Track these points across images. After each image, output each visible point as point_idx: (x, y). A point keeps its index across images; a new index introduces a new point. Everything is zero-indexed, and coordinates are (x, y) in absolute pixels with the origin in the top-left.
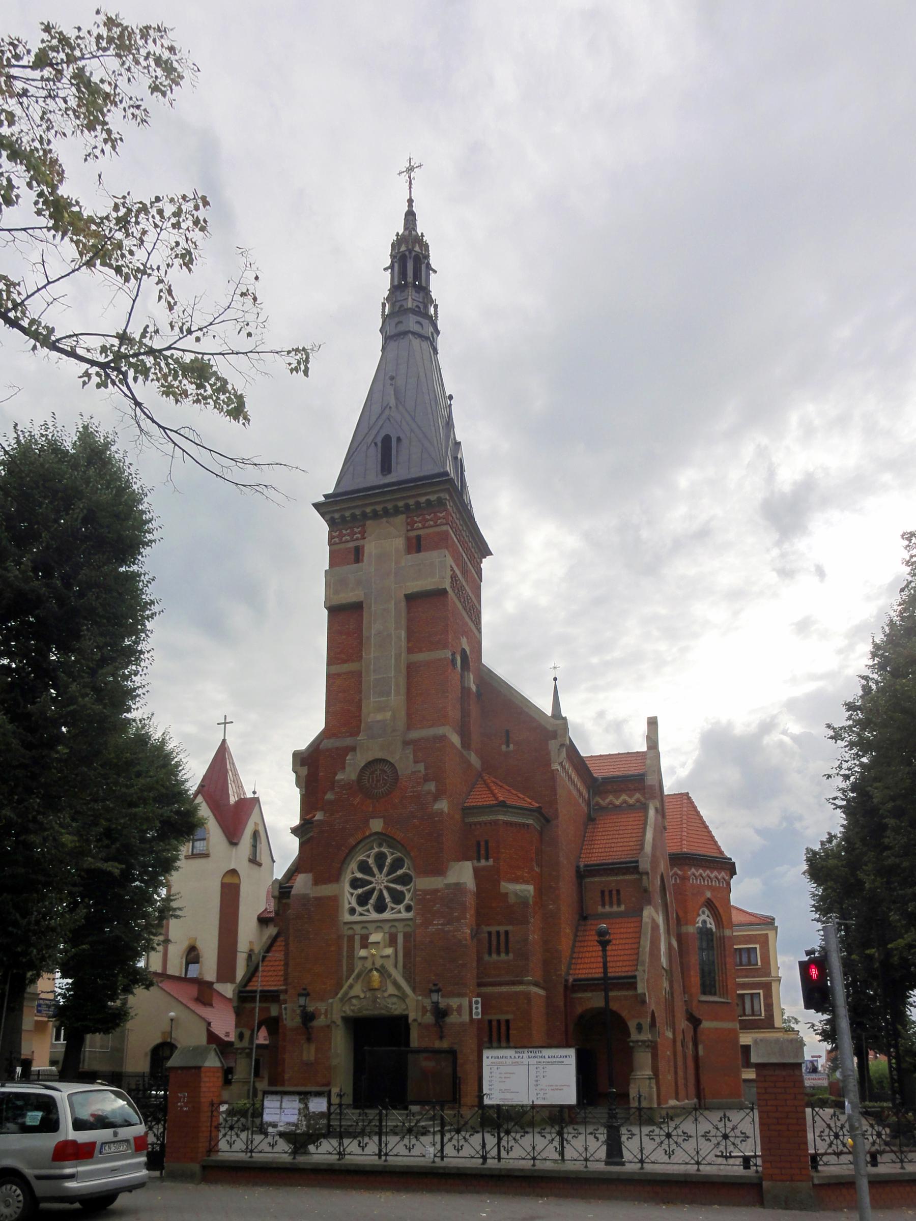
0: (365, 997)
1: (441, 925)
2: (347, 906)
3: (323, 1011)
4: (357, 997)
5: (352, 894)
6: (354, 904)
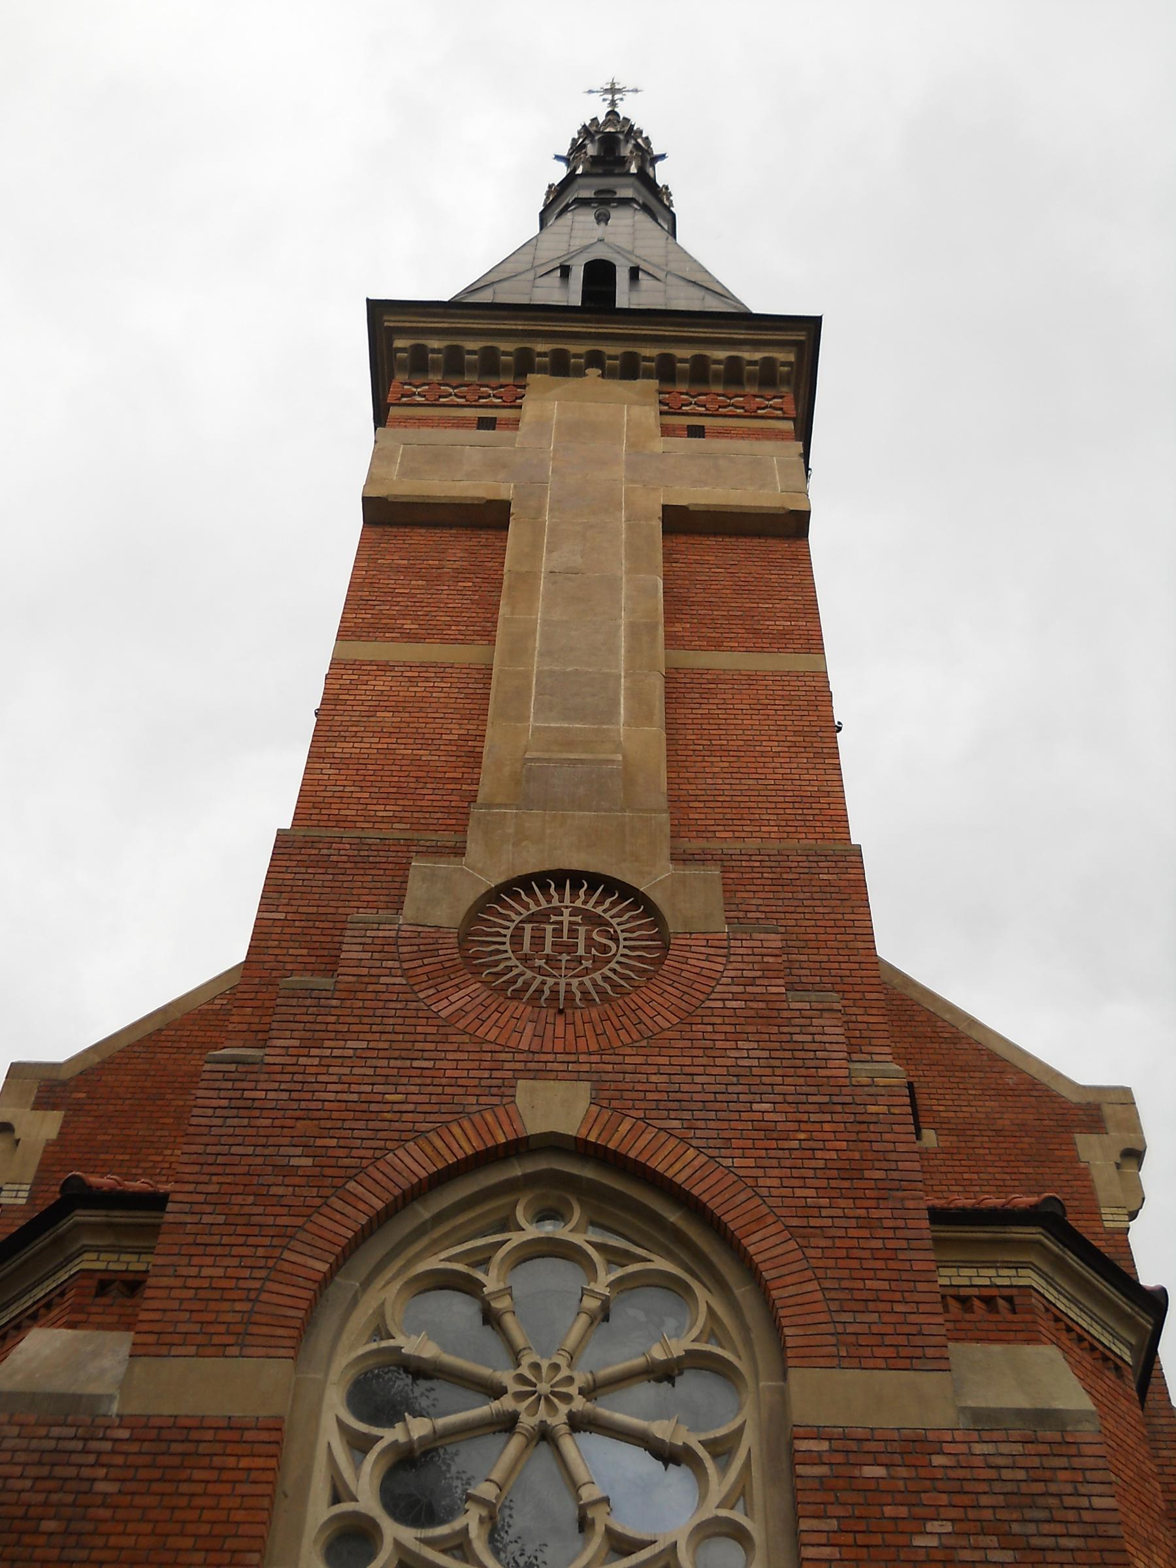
5: (359, 1445)
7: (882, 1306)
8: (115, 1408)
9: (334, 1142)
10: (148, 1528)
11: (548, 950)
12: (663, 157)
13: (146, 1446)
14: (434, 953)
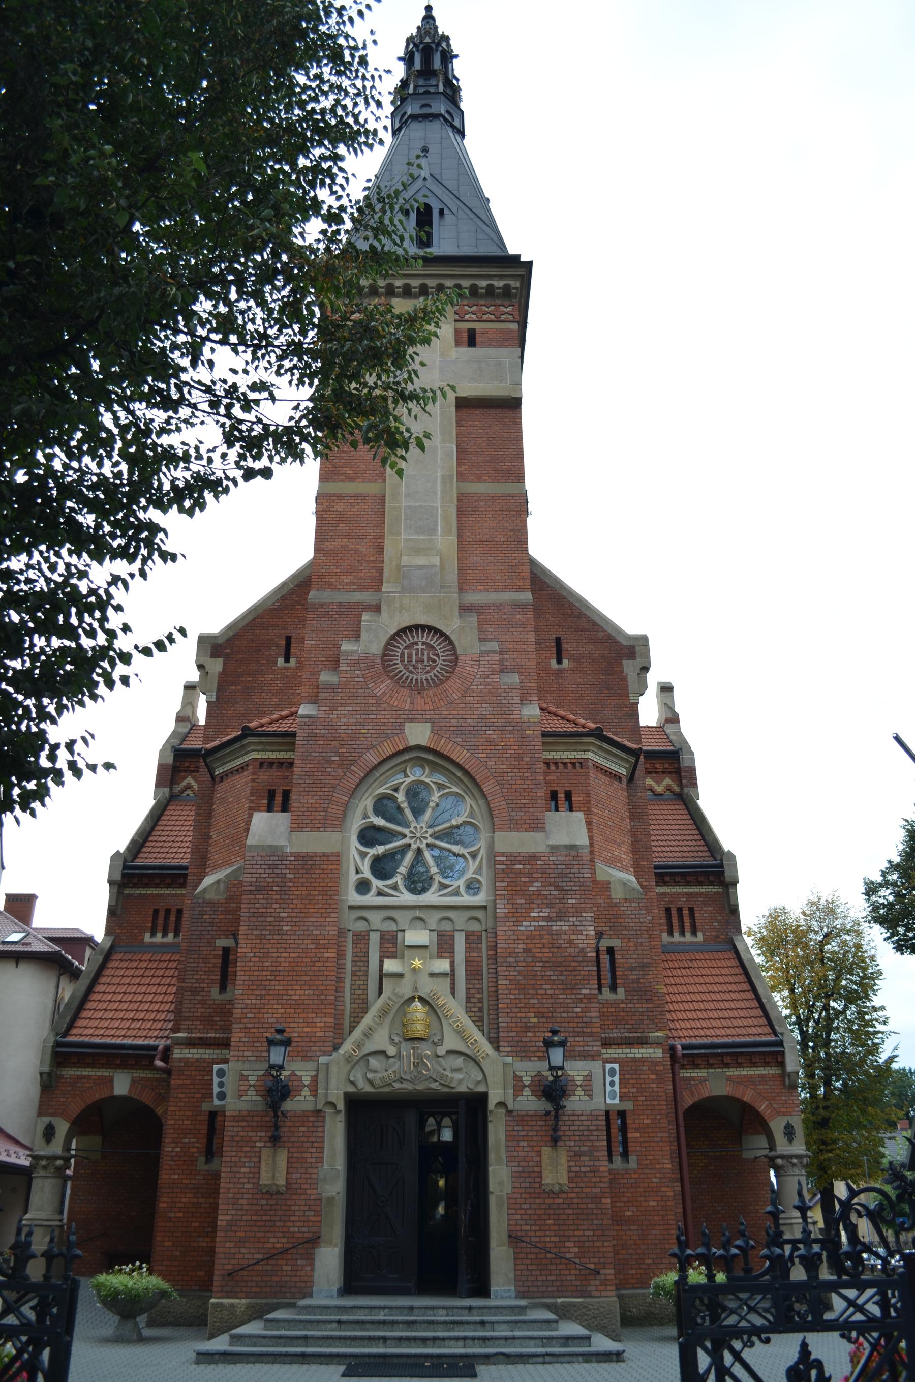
0: (398, 1056)
1: (548, 919)
2: (353, 878)
3: (307, 1080)
4: (384, 1053)
5: (363, 855)
6: (367, 873)
7: (526, 810)
8: (288, 850)
9: (345, 750)
10: (304, 889)
11: (414, 663)
12: (456, 56)
13: (300, 863)
14: (373, 666)
